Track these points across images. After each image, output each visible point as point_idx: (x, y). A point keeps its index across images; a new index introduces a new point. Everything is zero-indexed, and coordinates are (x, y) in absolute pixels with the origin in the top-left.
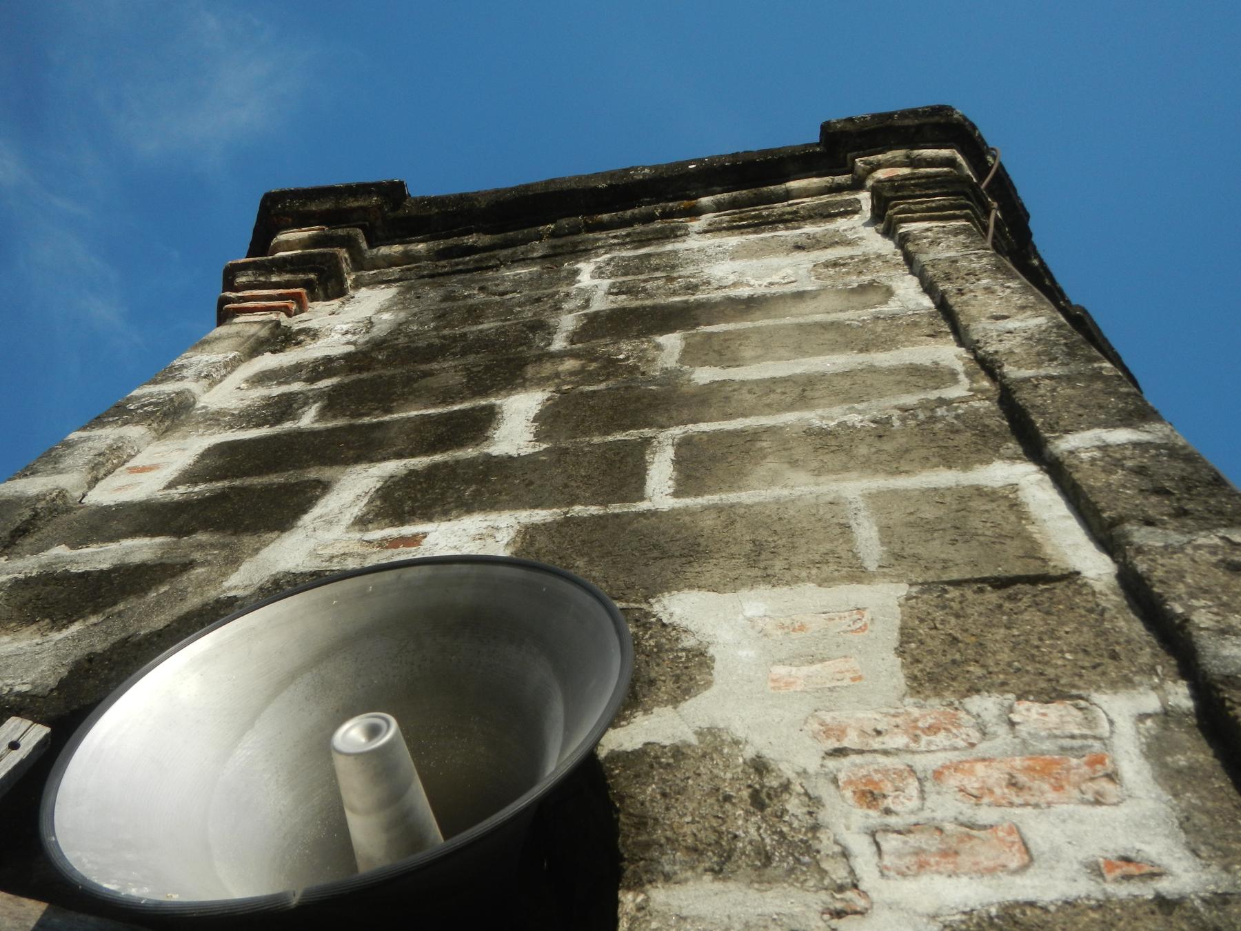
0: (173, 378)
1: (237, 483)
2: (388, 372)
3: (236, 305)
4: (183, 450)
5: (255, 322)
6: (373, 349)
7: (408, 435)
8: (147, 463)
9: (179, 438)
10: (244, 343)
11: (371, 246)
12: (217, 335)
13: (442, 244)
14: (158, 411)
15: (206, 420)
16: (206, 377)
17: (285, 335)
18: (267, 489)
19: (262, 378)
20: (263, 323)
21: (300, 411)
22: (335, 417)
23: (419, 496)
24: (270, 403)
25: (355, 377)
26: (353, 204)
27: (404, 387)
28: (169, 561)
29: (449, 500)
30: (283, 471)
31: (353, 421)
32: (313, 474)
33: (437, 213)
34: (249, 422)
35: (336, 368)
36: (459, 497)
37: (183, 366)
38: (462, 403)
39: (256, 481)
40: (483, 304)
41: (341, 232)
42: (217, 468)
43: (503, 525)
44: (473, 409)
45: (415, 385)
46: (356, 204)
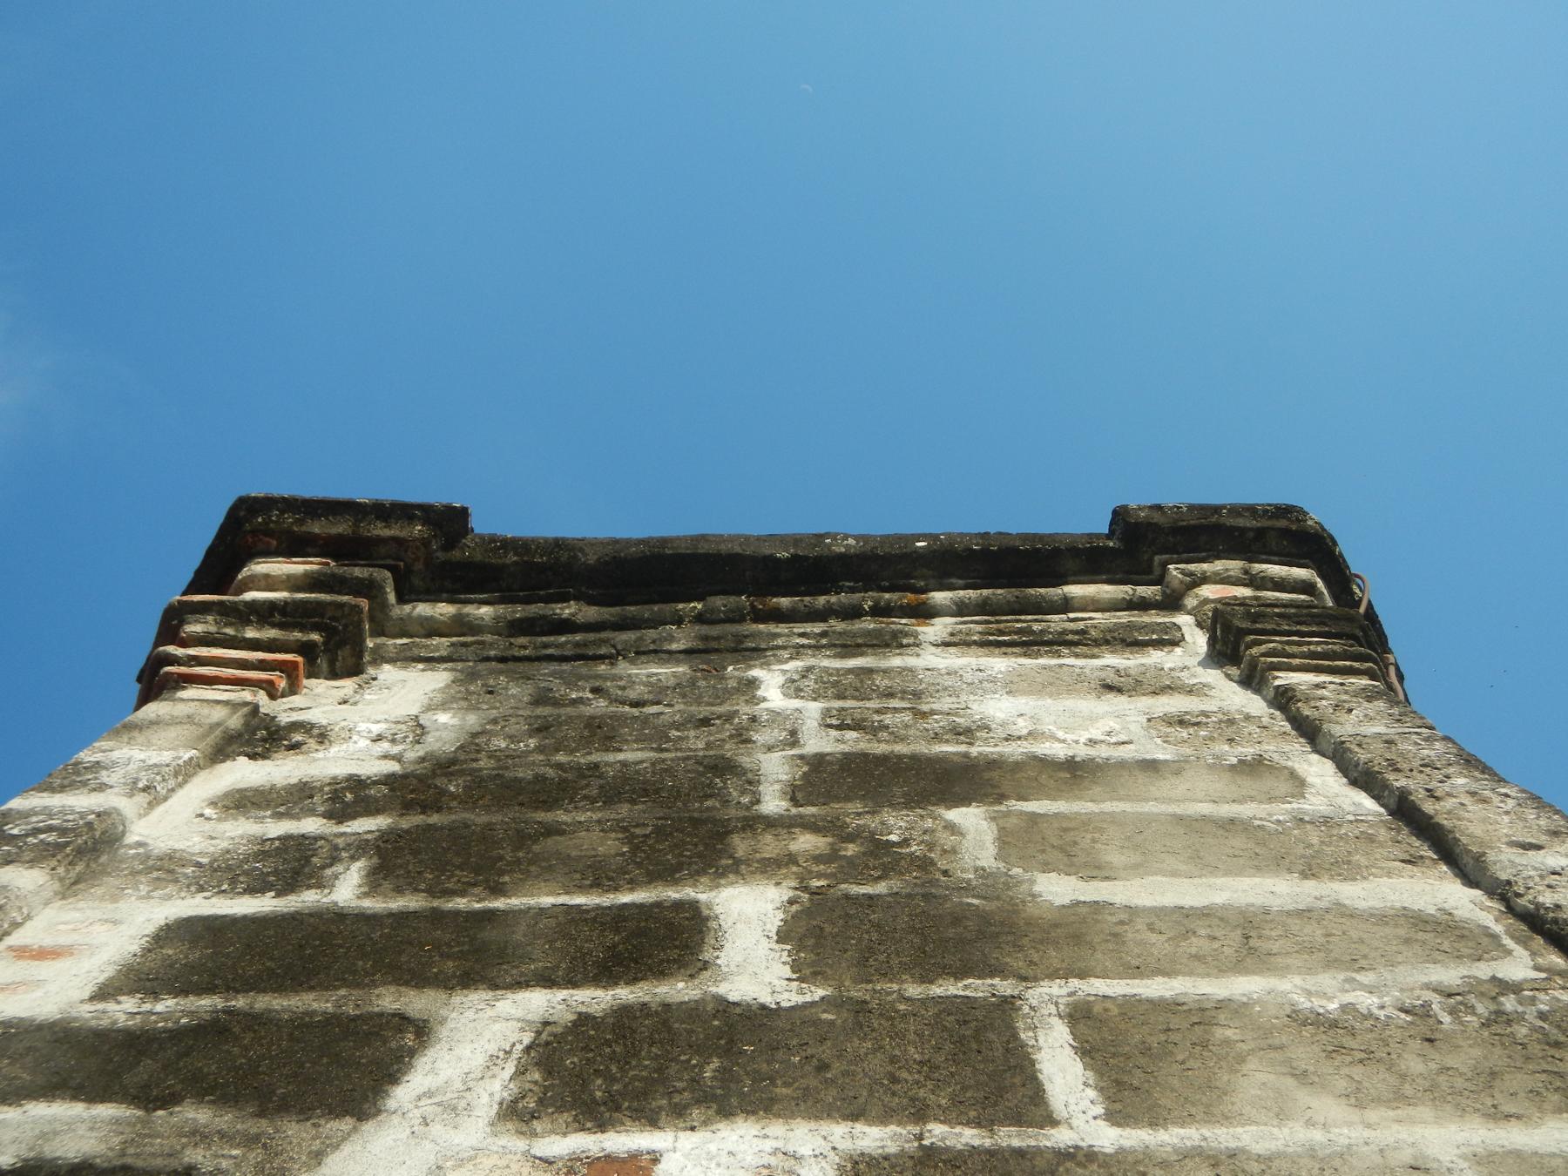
0: (84, 784)
1: (240, 1002)
2: (479, 818)
3: (183, 670)
4: (115, 922)
5: (218, 702)
6: (434, 775)
7: (551, 942)
8: (48, 941)
9: (102, 899)
10: (204, 736)
11: (402, 600)
12: (153, 716)
13: (519, 611)
14: (67, 844)
15: (149, 870)
16: (146, 789)
17: (266, 729)
18: (302, 1024)
19: (241, 802)
20: (234, 706)
21: (328, 872)
22: (399, 891)
23: (614, 1069)
24: (266, 850)
25: (417, 819)
26: (381, 530)
27: (516, 849)
28: (140, 1163)
29: (679, 1085)
30: (327, 987)
31: (436, 903)
32: (388, 1000)
33: (516, 563)
34: (233, 882)
35: (376, 800)
36: (693, 1080)
37: (97, 766)
38: (632, 890)
39: (265, 1002)
40: (610, 718)
41: (358, 572)
42: (191, 968)
43: (805, 1150)
44: (658, 904)
45: (536, 848)
46: (387, 533)
